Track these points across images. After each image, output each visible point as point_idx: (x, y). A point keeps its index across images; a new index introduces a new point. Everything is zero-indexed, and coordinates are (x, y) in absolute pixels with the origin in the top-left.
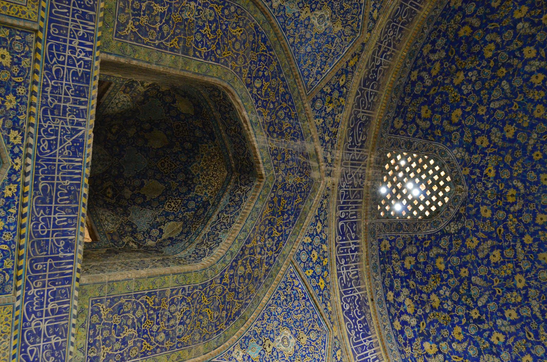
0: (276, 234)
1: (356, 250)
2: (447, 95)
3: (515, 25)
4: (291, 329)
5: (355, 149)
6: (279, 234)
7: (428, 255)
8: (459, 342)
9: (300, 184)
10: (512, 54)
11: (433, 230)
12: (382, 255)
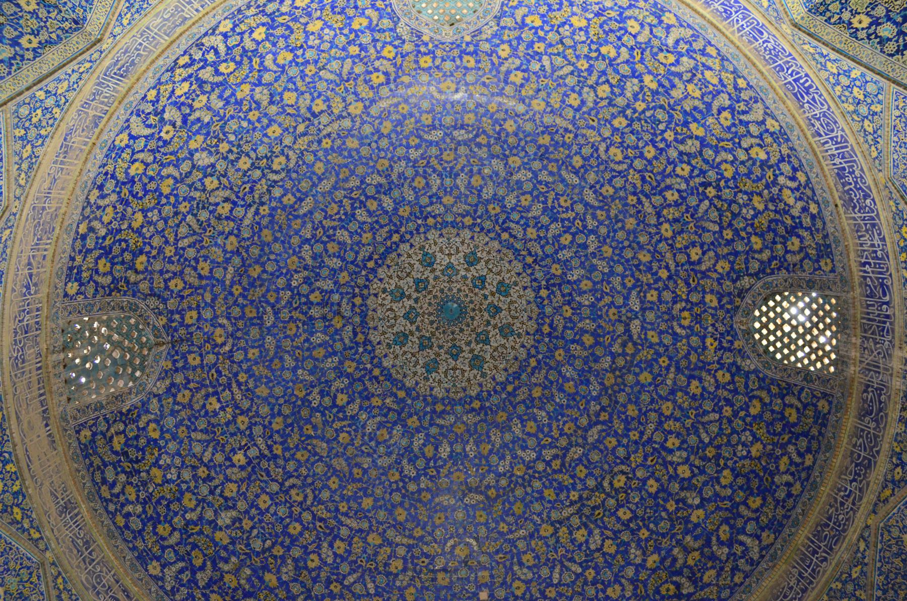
1: (864, 264)
2: (768, 432)
7: (772, 251)
8: (726, 161)
10: (702, 472)
11: (770, 279)
12: (830, 255)
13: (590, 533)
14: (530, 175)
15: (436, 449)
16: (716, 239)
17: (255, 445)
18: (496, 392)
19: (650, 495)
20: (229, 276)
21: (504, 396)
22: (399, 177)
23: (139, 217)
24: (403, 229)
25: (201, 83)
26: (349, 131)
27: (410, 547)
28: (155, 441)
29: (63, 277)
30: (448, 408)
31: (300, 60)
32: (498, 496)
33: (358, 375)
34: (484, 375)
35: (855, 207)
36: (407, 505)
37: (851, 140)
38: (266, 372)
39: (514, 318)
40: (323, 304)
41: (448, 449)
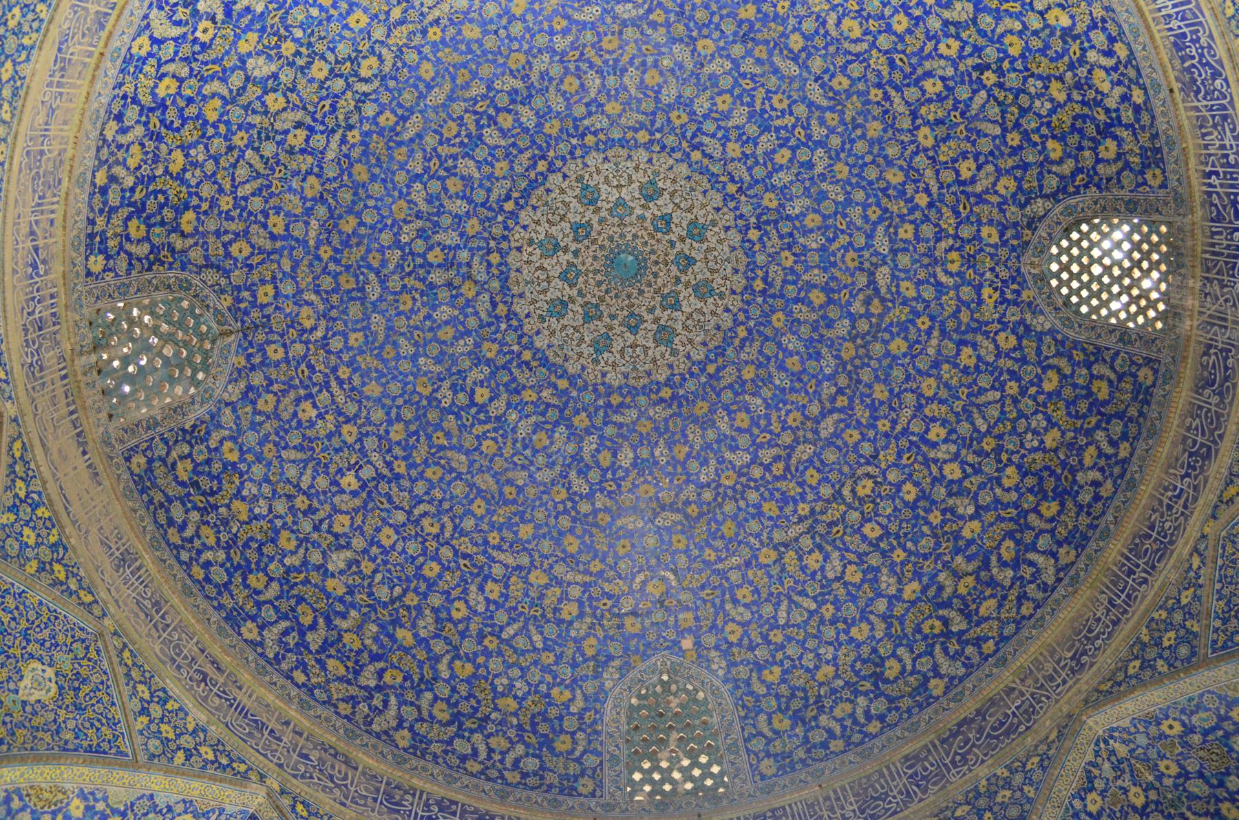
2: (1069, 414)
3: (977, 511)
5: (1220, 345)
7: (1077, 161)
8: (1011, 32)
12: (1160, 163)
13: (827, 558)
14: (728, 65)
15: (615, 455)
16: (997, 148)
17: (369, 462)
18: (692, 375)
19: (906, 504)
20: (312, 234)
21: (703, 380)
22: (542, 78)
23: (178, 156)
24: (551, 154)
26: (466, 13)
27: (586, 586)
28: (234, 464)
29: (82, 249)
30: (628, 400)
32: (701, 514)
33: (501, 361)
34: (674, 353)
35: (1198, 91)
36: (579, 531)
38: (376, 363)
39: (712, 271)
40: (447, 265)
41: (631, 455)
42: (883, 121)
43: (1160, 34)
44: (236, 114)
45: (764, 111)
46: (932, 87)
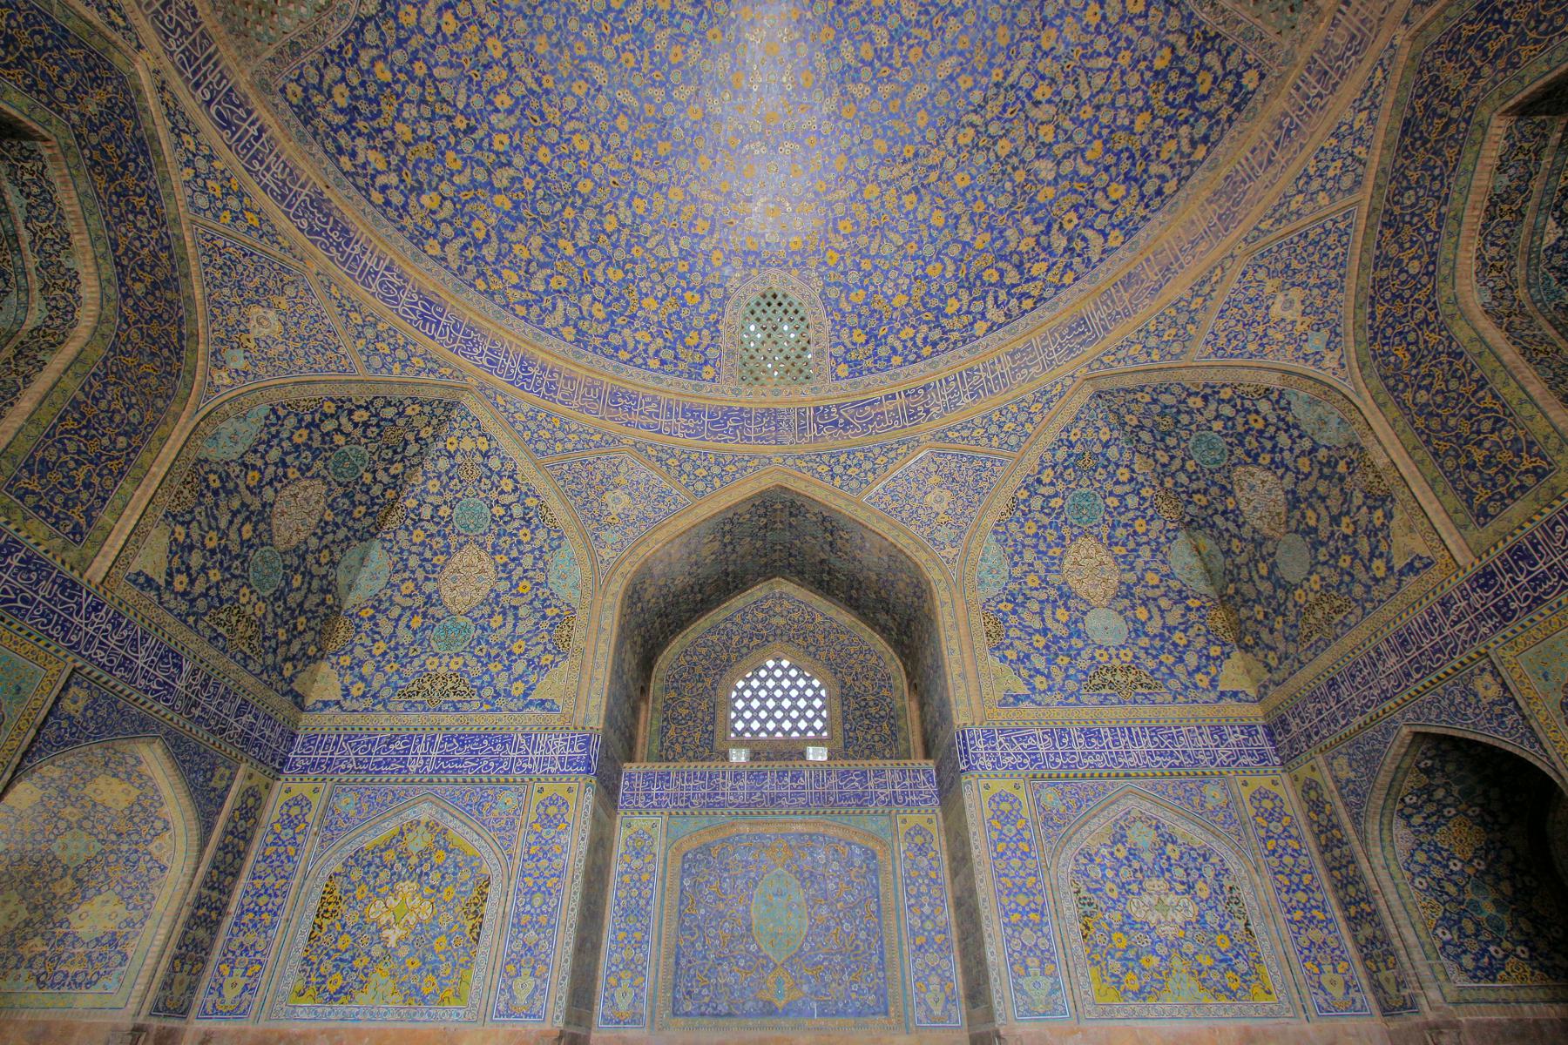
0: (140, 202)
1: (261, 130)
4: (258, 302)
6: (144, 199)
7: (359, 69)
8: (460, 172)
9: (109, 100)
11: (345, 24)
23: (1138, 128)
25: (1019, 267)
29: (1251, 104)
31: (920, 262)
37: (360, 288)
42: (535, 55)
43: (360, 230)
44: (1080, 137)
45: (641, 49)
46: (503, 101)
